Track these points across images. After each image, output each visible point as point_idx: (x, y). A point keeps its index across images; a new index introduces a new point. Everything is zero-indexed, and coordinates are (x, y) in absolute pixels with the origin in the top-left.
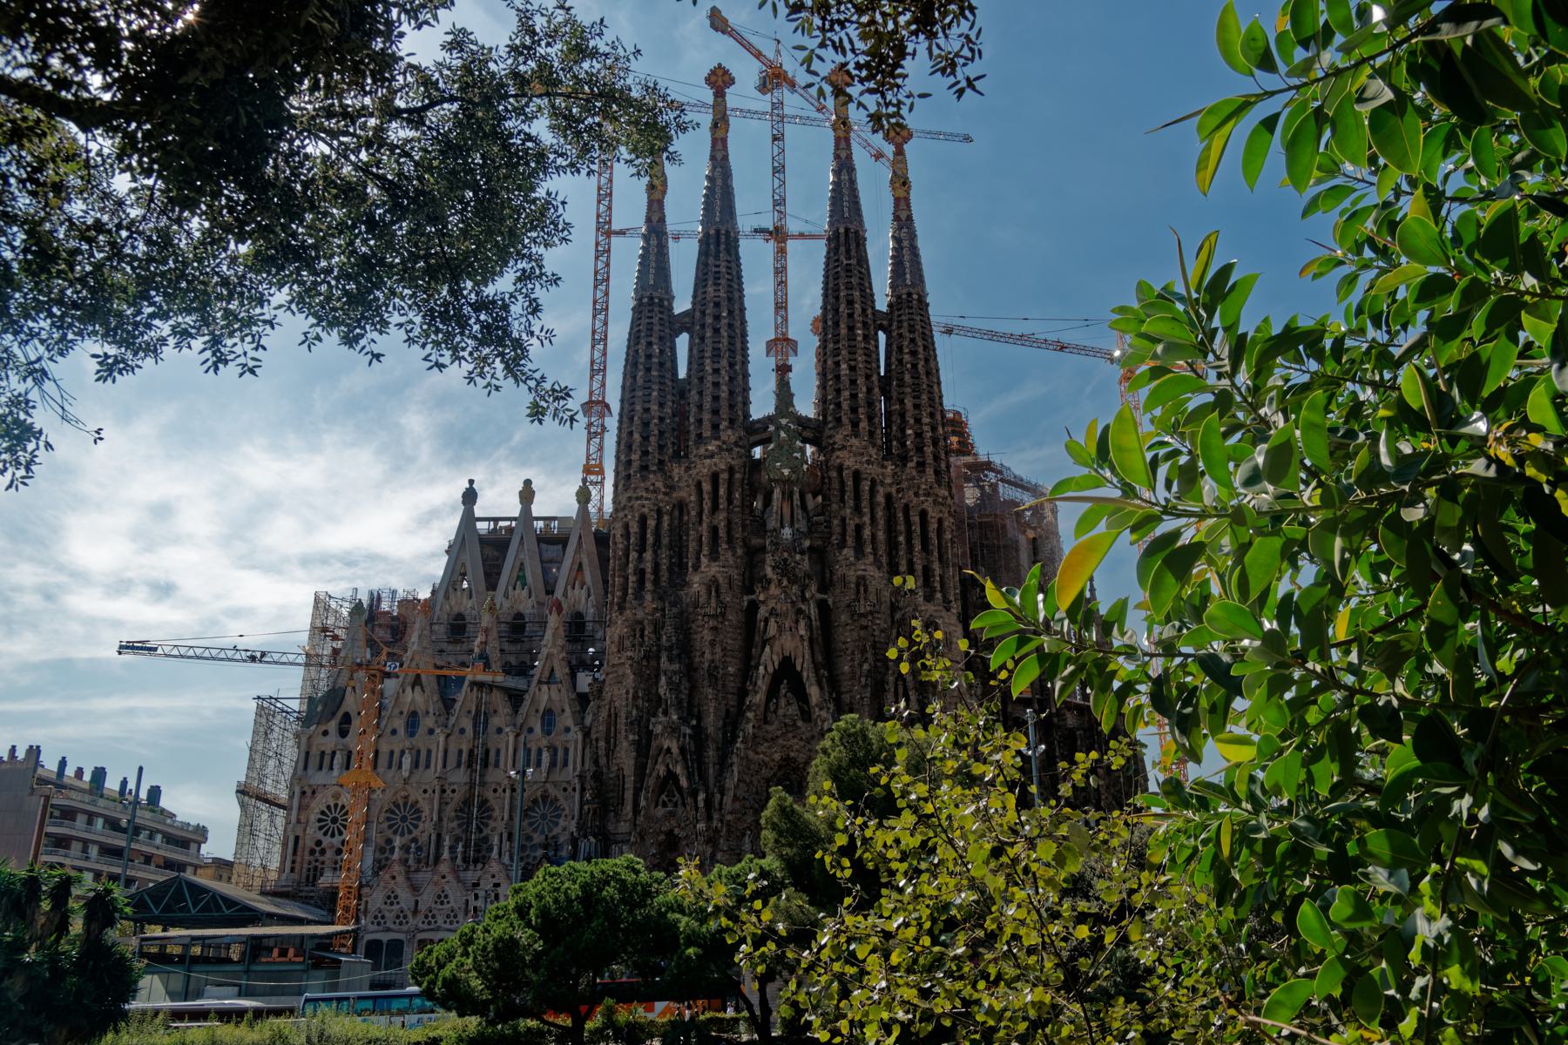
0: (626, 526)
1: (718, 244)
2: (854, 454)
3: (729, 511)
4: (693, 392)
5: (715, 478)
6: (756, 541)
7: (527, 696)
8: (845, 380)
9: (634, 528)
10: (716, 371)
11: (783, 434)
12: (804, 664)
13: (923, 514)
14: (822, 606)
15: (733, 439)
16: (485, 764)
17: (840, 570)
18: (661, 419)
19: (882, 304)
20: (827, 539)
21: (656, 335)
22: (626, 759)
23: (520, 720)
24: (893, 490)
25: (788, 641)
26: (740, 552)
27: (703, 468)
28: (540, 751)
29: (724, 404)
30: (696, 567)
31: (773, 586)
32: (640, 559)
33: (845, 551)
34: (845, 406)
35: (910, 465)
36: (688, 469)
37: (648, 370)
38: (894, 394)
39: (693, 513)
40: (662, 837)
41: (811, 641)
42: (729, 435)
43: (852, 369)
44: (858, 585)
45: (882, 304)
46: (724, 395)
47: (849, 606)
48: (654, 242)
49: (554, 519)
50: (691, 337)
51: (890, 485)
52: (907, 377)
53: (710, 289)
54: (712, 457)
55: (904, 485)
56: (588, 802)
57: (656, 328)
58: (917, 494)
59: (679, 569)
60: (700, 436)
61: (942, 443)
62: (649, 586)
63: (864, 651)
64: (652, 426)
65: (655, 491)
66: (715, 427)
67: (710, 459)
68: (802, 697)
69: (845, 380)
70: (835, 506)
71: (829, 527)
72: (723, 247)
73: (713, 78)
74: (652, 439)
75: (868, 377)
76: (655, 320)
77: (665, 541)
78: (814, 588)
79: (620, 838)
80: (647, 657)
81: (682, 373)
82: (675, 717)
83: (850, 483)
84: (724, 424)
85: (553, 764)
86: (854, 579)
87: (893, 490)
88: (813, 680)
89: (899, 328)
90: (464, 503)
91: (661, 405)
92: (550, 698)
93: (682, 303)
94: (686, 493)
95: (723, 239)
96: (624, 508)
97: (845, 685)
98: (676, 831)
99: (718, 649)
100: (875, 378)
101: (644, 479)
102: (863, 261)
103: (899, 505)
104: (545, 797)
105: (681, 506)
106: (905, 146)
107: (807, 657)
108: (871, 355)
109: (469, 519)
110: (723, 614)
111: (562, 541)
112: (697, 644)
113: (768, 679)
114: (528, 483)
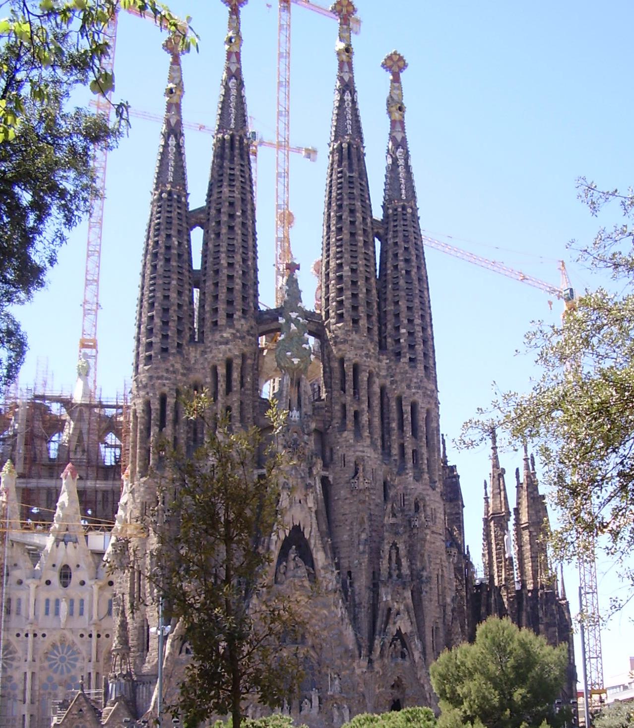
1: (232, 148)
3: (243, 394)
9: (155, 406)
10: (231, 265)
11: (293, 326)
12: (311, 533)
13: (414, 406)
14: (324, 480)
15: (245, 328)
16: (8, 612)
17: (340, 451)
18: (180, 306)
19: (378, 214)
20: (328, 423)
24: (388, 383)
27: (219, 354)
28: (57, 602)
29: (238, 296)
33: (345, 434)
35: (402, 360)
37: (168, 260)
38: (389, 296)
41: (316, 512)
42: (242, 324)
43: (353, 271)
44: (356, 465)
45: (378, 214)
46: (238, 287)
47: (348, 482)
48: (172, 142)
50: (206, 233)
51: (385, 377)
53: (225, 190)
54: (227, 343)
55: (398, 378)
58: (409, 387)
60: (215, 323)
63: (362, 523)
64: (171, 312)
65: (174, 372)
66: (230, 316)
69: (347, 280)
72: (237, 152)
76: (174, 215)
78: (319, 463)
81: (197, 265)
84: (237, 315)
86: (353, 460)
87: (388, 383)
89: (394, 237)
91: (180, 293)
93: (197, 199)
94: (203, 376)
95: (237, 144)
96: (145, 387)
97: (344, 552)
100: (373, 280)
101: (164, 359)
102: (363, 175)
103: (392, 396)
104: (63, 642)
106: (401, 74)
107: (315, 526)
108: (369, 259)
113: (280, 544)
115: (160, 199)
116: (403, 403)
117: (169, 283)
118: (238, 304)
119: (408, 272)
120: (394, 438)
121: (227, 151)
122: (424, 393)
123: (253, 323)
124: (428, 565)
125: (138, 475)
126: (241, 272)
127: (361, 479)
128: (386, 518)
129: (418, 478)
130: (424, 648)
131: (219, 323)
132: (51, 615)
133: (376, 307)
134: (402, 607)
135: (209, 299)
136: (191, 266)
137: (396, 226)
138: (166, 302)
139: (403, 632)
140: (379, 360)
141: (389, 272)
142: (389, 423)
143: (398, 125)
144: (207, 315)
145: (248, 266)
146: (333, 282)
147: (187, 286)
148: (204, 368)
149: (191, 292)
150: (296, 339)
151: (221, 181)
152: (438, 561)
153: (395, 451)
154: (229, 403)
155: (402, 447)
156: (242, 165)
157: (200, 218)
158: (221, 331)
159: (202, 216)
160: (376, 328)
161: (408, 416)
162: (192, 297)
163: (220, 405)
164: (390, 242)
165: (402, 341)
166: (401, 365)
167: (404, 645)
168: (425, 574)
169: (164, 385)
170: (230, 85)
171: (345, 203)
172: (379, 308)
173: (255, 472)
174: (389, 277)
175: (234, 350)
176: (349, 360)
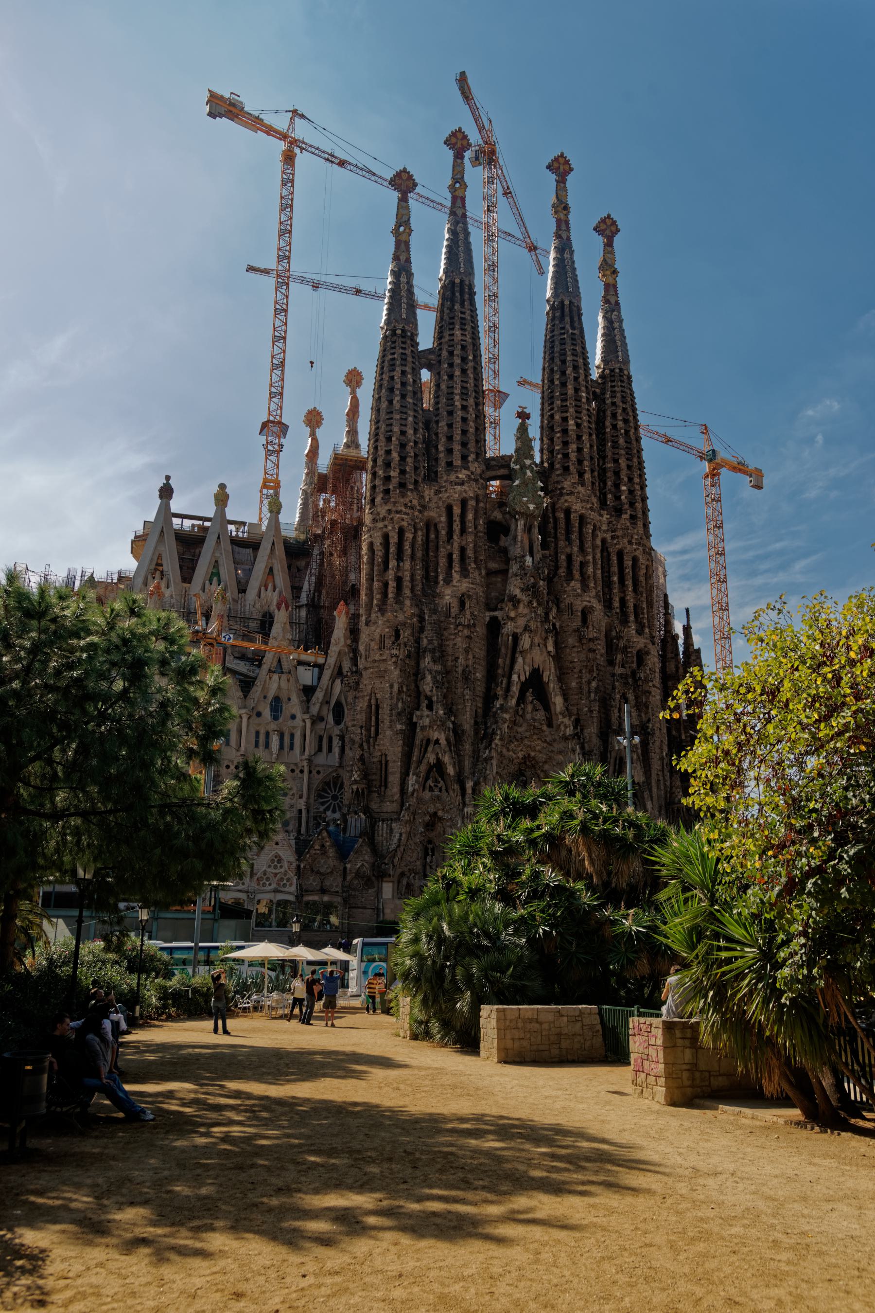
0: (386, 537)
1: (462, 293)
2: (579, 499)
3: (476, 535)
4: (442, 424)
5: (464, 503)
7: (257, 682)
8: (572, 434)
9: (394, 539)
10: (464, 408)
11: (529, 473)
12: (549, 675)
13: (635, 560)
15: (479, 471)
17: (567, 599)
18: (416, 443)
19: (595, 374)
22: (390, 745)
23: (251, 703)
24: (608, 536)
25: (535, 655)
26: (483, 572)
27: (454, 494)
29: (472, 438)
30: (448, 581)
31: (521, 605)
33: (573, 583)
34: (573, 457)
35: (624, 516)
36: (438, 492)
37: (403, 396)
38: (609, 454)
39: (443, 532)
40: (427, 818)
43: (578, 425)
45: (595, 374)
47: (577, 630)
49: (244, 524)
52: (621, 441)
53: (458, 333)
54: (462, 484)
55: (619, 533)
56: (356, 782)
57: (410, 359)
58: (630, 542)
59: (430, 580)
60: (450, 464)
62: (407, 592)
64: (408, 448)
65: (412, 508)
66: (464, 458)
67: (457, 487)
68: (546, 705)
69: (572, 434)
70: (562, 543)
73: (454, 140)
74: (410, 460)
75: (590, 435)
79: (385, 816)
80: (408, 656)
82: (441, 712)
84: (472, 457)
85: (281, 747)
86: (580, 609)
87: (608, 536)
88: (558, 691)
90: (161, 497)
91: (416, 431)
92: (279, 687)
93: (426, 340)
96: (384, 519)
98: (440, 813)
99: (470, 657)
101: (403, 495)
105: (430, 525)
107: (553, 670)
109: (165, 514)
110: (474, 625)
111: (252, 545)
112: (450, 650)
114: (222, 486)
116: (625, 558)
117: (406, 419)
120: (615, 591)
121: (457, 294)
129: (640, 632)
131: (455, 464)
132: (261, 747)
138: (402, 438)
140: (601, 516)
141: (608, 430)
143: (611, 289)
144: (441, 455)
148: (438, 507)
150: (530, 486)
151: (453, 324)
153: (616, 604)
154: (464, 543)
155: (623, 602)
157: (430, 359)
158: (456, 472)
159: (432, 357)
161: (628, 571)
163: (456, 545)
164: (608, 401)
166: (622, 521)
169: (403, 520)
170: (458, 229)
173: (487, 614)
175: (470, 491)
176: (576, 511)
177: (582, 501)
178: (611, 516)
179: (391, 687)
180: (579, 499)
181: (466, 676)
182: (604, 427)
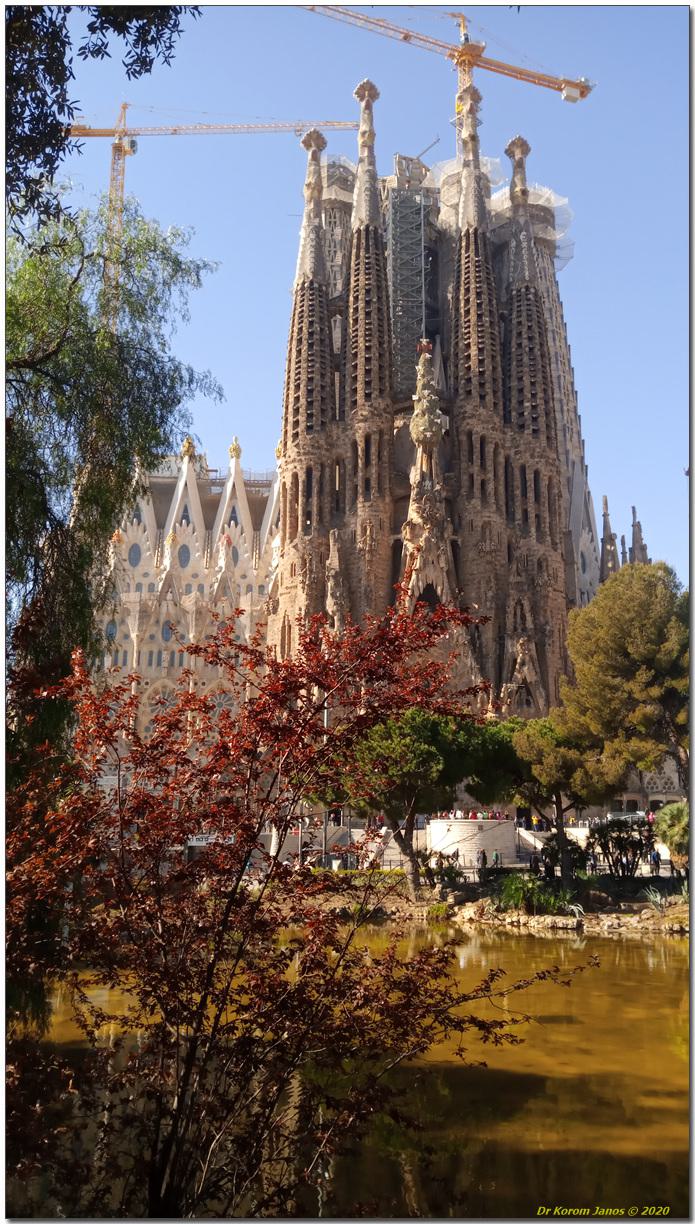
0: (295, 476)
2: (481, 420)
4: (348, 366)
5: (367, 439)
6: (400, 492)
9: (302, 477)
13: (537, 473)
14: (454, 544)
15: (382, 406)
17: (468, 517)
18: (323, 387)
21: (317, 314)
26: (388, 499)
27: (360, 430)
32: (307, 503)
33: (473, 501)
34: (475, 381)
35: (526, 432)
37: (311, 346)
38: (514, 373)
39: (349, 467)
43: (481, 350)
51: (510, 448)
55: (522, 448)
58: (532, 456)
61: (552, 415)
63: (488, 582)
65: (319, 448)
70: (464, 465)
71: (459, 480)
75: (493, 357)
77: (327, 489)
78: (450, 528)
83: (477, 445)
86: (480, 524)
87: (513, 451)
89: (518, 317)
91: (323, 376)
95: (372, 235)
105: (339, 461)
107: (446, 584)
112: (354, 573)
115: (303, 289)
116: (527, 471)
118: (375, 384)
119: (531, 349)
120: (517, 504)
122: (546, 461)
123: (389, 401)
124: (550, 620)
125: (288, 541)
126: (377, 355)
127: (488, 541)
128: (512, 577)
129: (540, 539)
130: (548, 696)
133: (501, 384)
134: (527, 658)
135: (349, 381)
136: (332, 350)
137: (520, 306)
139: (529, 681)
140: (504, 433)
141: (513, 350)
142: (513, 491)
145: (384, 349)
146: (462, 361)
147: (328, 369)
149: (333, 374)
152: (560, 616)
153: (519, 515)
155: (525, 513)
156: (377, 254)
160: (501, 403)
161: (531, 484)
162: (333, 380)
164: (514, 322)
165: (526, 414)
166: (525, 436)
167: (529, 693)
168: (548, 628)
171: (472, 286)
172: (504, 385)
174: (514, 356)
176: (477, 433)
177: (483, 422)
178: (515, 433)
179: (300, 609)
180: (481, 420)
181: (368, 594)
182: (510, 348)
